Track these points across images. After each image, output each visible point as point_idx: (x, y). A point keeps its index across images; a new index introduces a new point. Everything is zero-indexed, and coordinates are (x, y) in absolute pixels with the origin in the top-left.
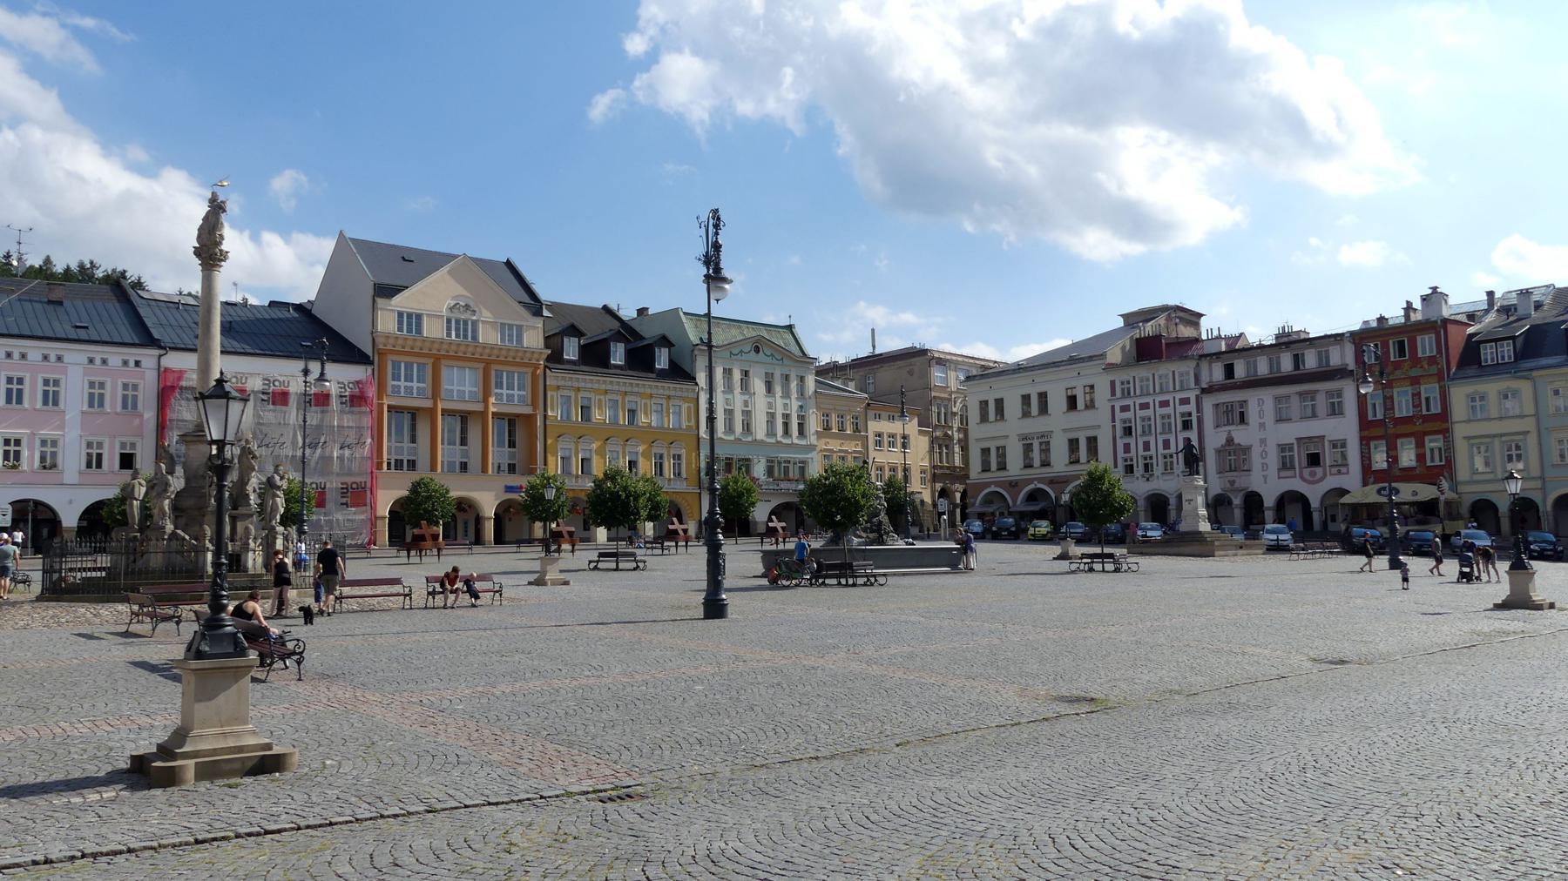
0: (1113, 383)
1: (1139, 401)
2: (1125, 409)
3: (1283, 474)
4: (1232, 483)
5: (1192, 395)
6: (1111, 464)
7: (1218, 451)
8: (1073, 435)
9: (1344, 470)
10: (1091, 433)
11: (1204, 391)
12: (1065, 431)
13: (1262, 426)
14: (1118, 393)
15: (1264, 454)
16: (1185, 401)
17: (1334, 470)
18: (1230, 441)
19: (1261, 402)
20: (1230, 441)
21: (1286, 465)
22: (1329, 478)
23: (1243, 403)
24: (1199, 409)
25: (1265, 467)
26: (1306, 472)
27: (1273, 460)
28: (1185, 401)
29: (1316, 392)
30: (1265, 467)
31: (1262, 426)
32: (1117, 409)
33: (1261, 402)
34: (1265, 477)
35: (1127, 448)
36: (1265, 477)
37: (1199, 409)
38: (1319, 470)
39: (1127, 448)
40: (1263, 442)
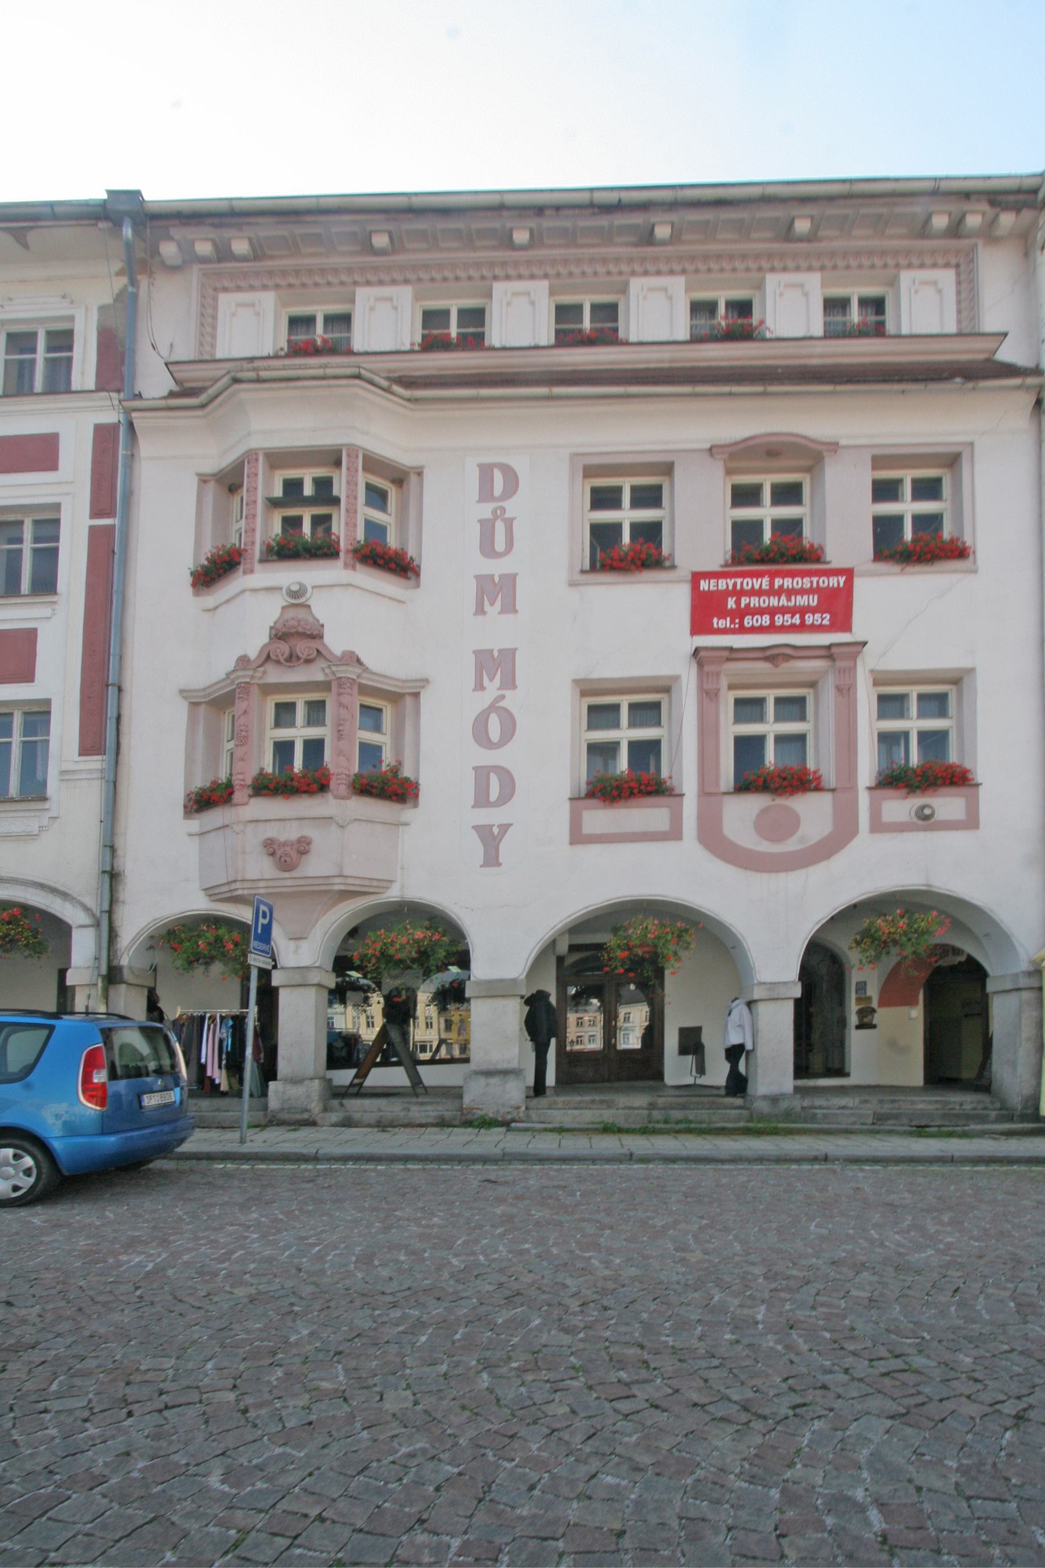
3: (601, 818)
13: (497, 593)
15: (494, 727)
17: (900, 807)
19: (497, 482)
21: (625, 781)
22: (865, 845)
23: (391, 481)
24: (109, 492)
25: (493, 786)
26: (741, 815)
27: (551, 754)
30: (493, 786)
31: (497, 593)
33: (497, 482)
34: (491, 840)
36: (491, 840)
37: (109, 492)
38: (813, 812)
40: (496, 665)
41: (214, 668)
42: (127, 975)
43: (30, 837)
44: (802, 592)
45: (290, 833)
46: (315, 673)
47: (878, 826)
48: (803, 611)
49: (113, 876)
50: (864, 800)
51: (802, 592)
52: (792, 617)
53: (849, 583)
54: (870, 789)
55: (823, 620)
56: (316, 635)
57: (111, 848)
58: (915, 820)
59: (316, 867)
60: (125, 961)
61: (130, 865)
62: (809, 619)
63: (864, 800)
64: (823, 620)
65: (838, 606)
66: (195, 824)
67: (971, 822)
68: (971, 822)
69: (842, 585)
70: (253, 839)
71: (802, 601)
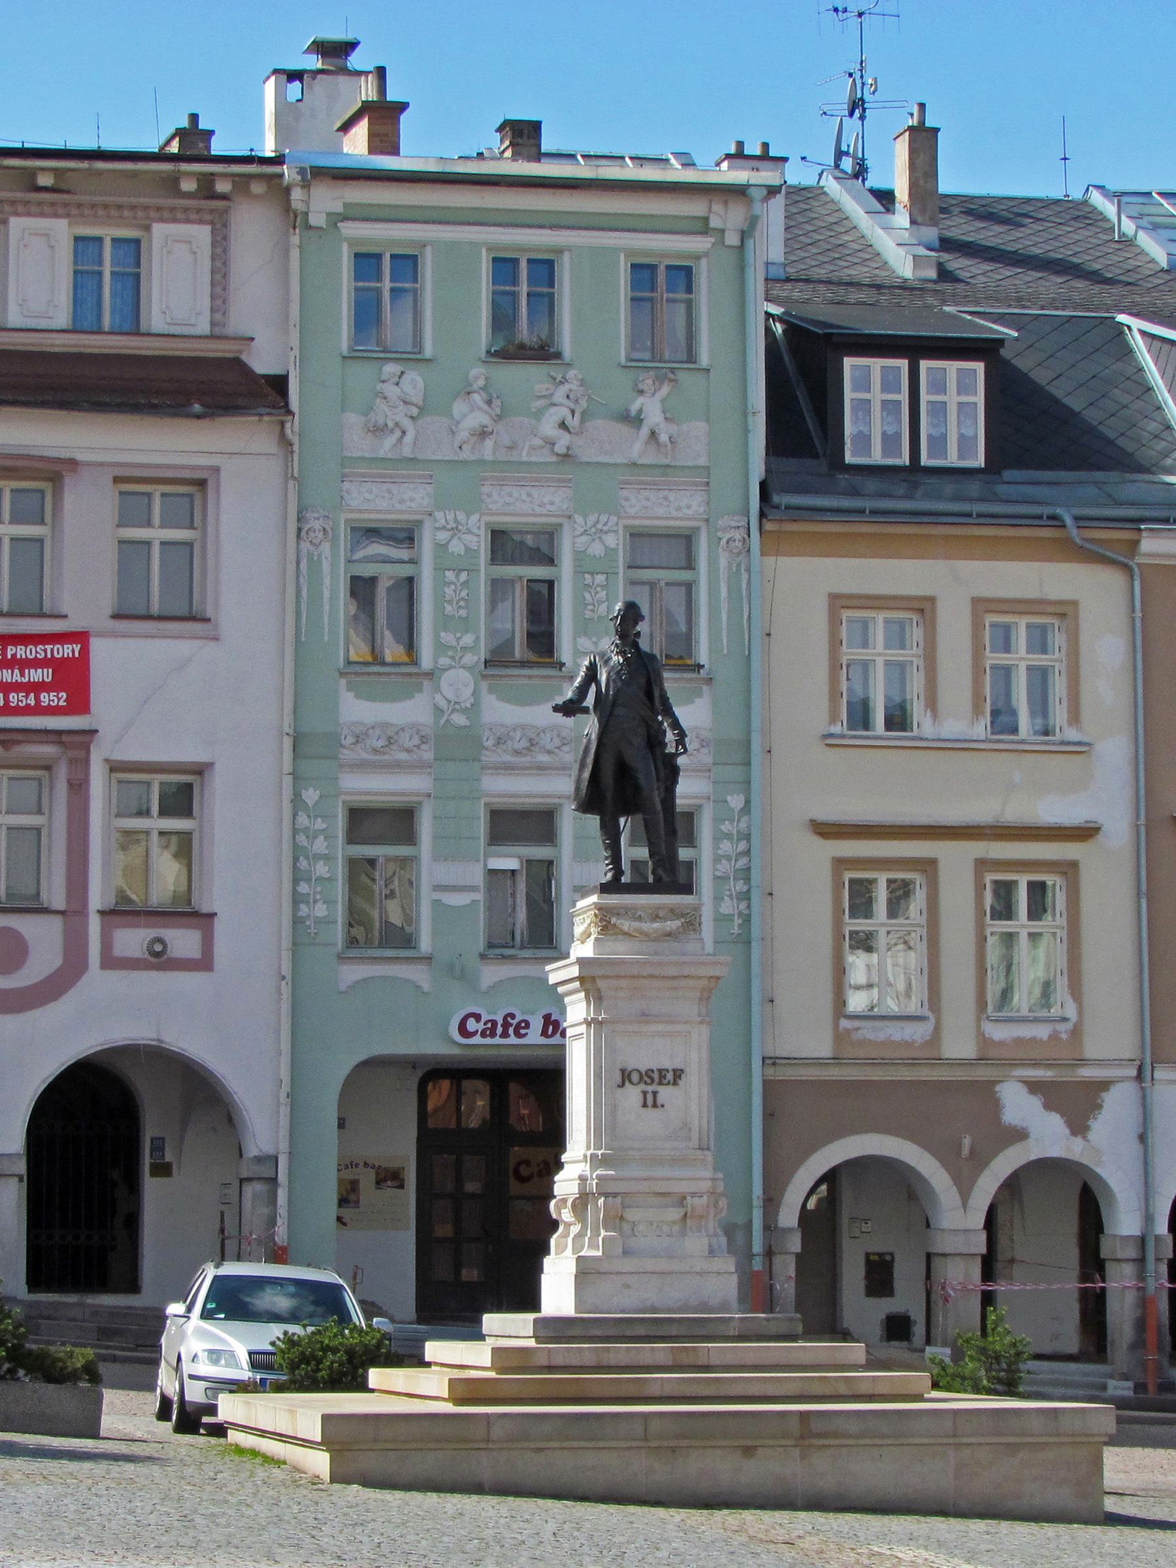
9: (183, 941)
17: (132, 940)
22: (97, 981)
29: (55, 472)
44: (36, 663)
47: (110, 962)
48: (36, 688)
50: (94, 925)
51: (36, 663)
52: (27, 697)
53: (85, 651)
54: (101, 913)
55: (59, 699)
58: (147, 956)
62: (45, 698)
63: (94, 925)
64: (59, 699)
65: (74, 680)
67: (204, 963)
68: (204, 963)
69: (77, 655)
71: (36, 675)
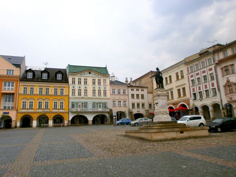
0: (188, 68)
1: (196, 73)
2: (192, 76)
4: (231, 98)
5: (213, 67)
6: (189, 97)
7: (225, 86)
8: (178, 88)
10: (183, 87)
11: (216, 64)
12: (176, 87)
14: (190, 72)
16: (210, 70)
18: (228, 81)
20: (228, 81)
24: (216, 72)
28: (210, 70)
32: (190, 77)
35: (194, 89)
37: (216, 72)
39: (194, 89)
41: (224, 84)
42: (224, 108)
43: (216, 98)
45: (231, 97)
46: (230, 84)
49: (221, 101)
56: (229, 81)
57: (221, 99)
59: (233, 99)
60: (224, 107)
61: (223, 100)
66: (226, 96)
70: (228, 97)
